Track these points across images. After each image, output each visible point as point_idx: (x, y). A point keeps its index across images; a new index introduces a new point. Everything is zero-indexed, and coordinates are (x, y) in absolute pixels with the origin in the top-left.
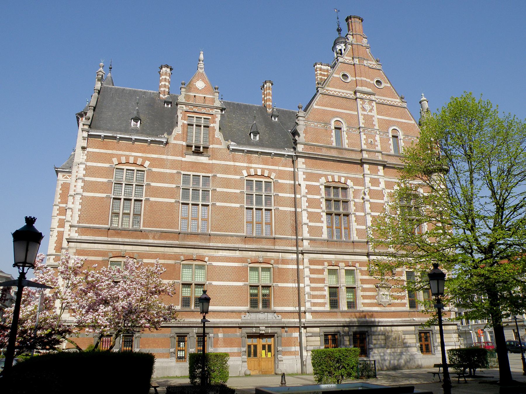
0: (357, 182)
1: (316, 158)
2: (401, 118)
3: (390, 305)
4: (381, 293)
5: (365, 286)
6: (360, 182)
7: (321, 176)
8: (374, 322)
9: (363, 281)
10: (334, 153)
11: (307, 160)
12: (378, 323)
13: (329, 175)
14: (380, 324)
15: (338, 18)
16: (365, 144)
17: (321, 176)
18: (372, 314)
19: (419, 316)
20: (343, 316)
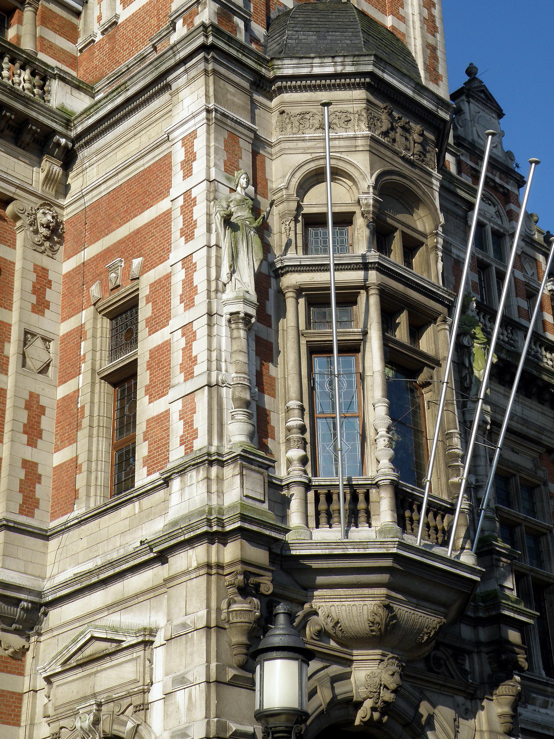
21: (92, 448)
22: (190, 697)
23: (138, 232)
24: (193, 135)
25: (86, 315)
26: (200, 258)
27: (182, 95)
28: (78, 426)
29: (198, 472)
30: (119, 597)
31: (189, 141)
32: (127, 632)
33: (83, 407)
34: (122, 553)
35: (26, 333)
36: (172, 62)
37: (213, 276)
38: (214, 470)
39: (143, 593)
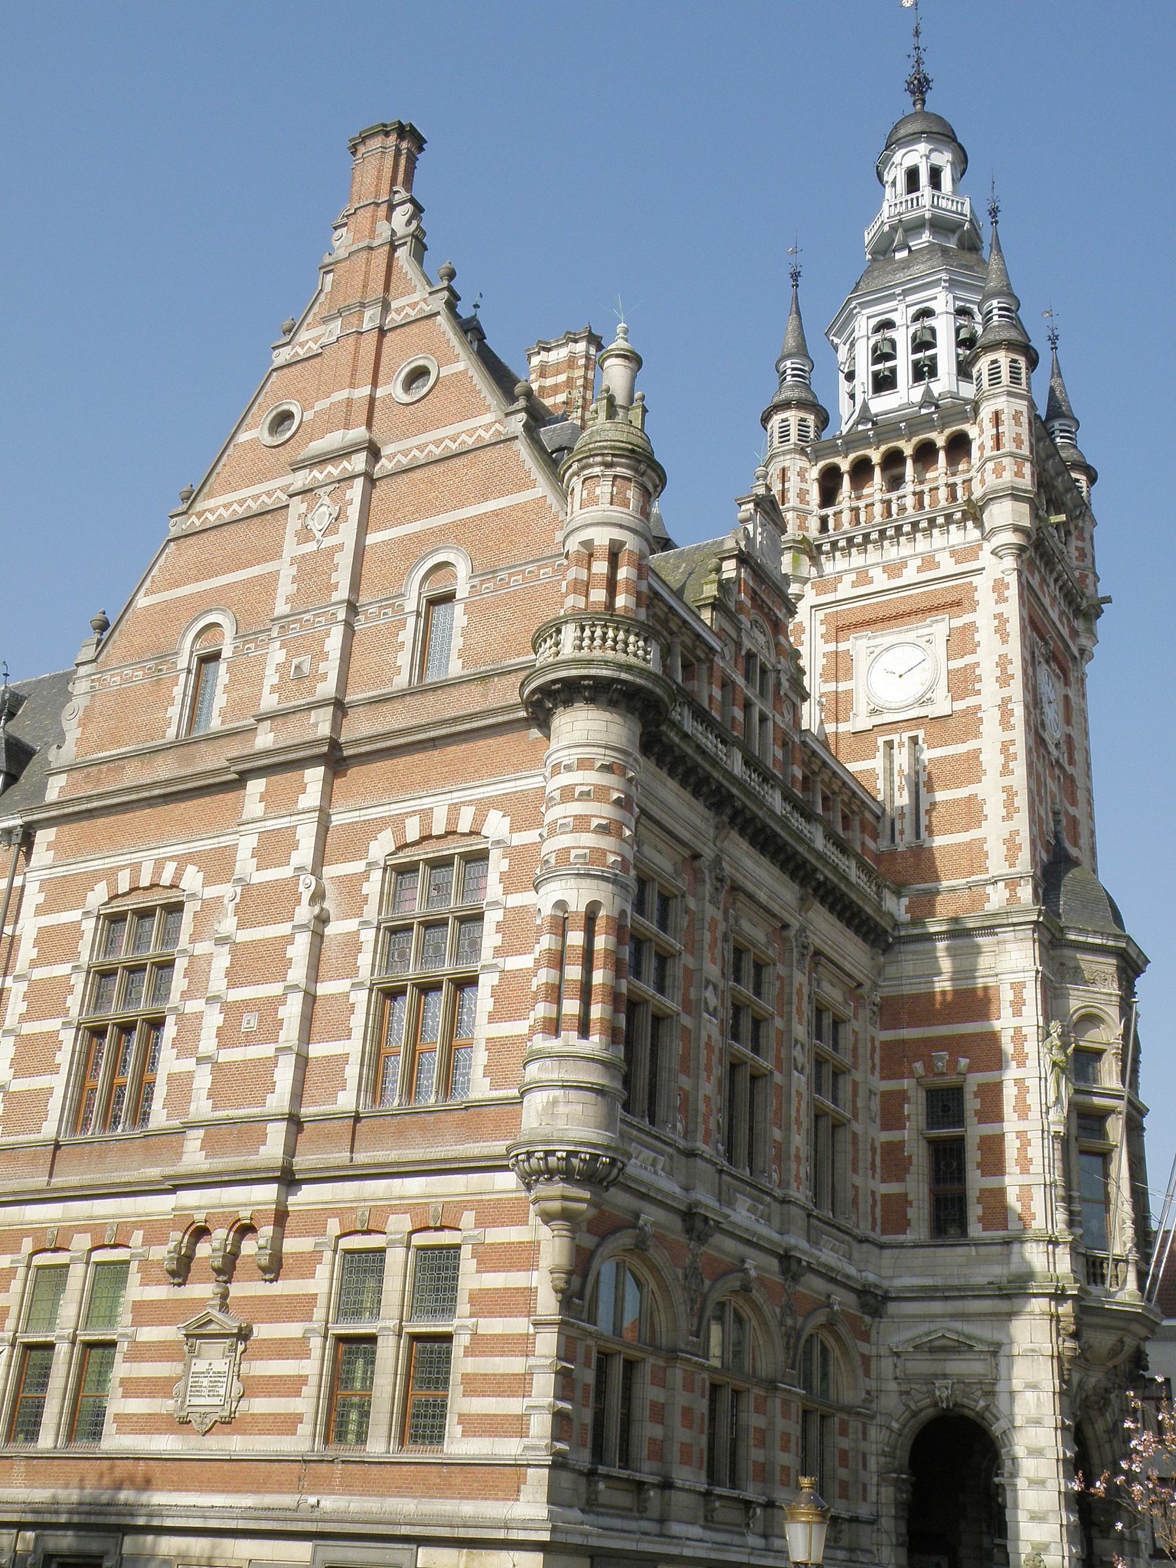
0: (218, 865)
1: (90, 814)
2: (485, 498)
3: (228, 1423)
4: (199, 1366)
5: (148, 1334)
6: (218, 865)
7: (93, 878)
8: (130, 1509)
9: (145, 1313)
10: (164, 769)
11: (66, 828)
12: (150, 1516)
13: (122, 868)
14: (156, 1522)
15: (917, 34)
16: (274, 689)
17: (93, 878)
18: (150, 1471)
19: (347, 1489)
20: (31, 1480)
21: (917, 1187)
22: (1039, 1398)
23: (962, 1036)
24: (1023, 985)
25: (906, 1084)
26: (1032, 1084)
27: (1009, 946)
28: (907, 1171)
29: (1038, 1246)
30: (959, 1311)
31: (1018, 987)
32: (980, 1341)
33: (910, 1157)
34: (963, 1282)
35: (870, 1091)
36: (1005, 922)
37: (1043, 1102)
38: (1051, 1247)
39: (985, 1314)
